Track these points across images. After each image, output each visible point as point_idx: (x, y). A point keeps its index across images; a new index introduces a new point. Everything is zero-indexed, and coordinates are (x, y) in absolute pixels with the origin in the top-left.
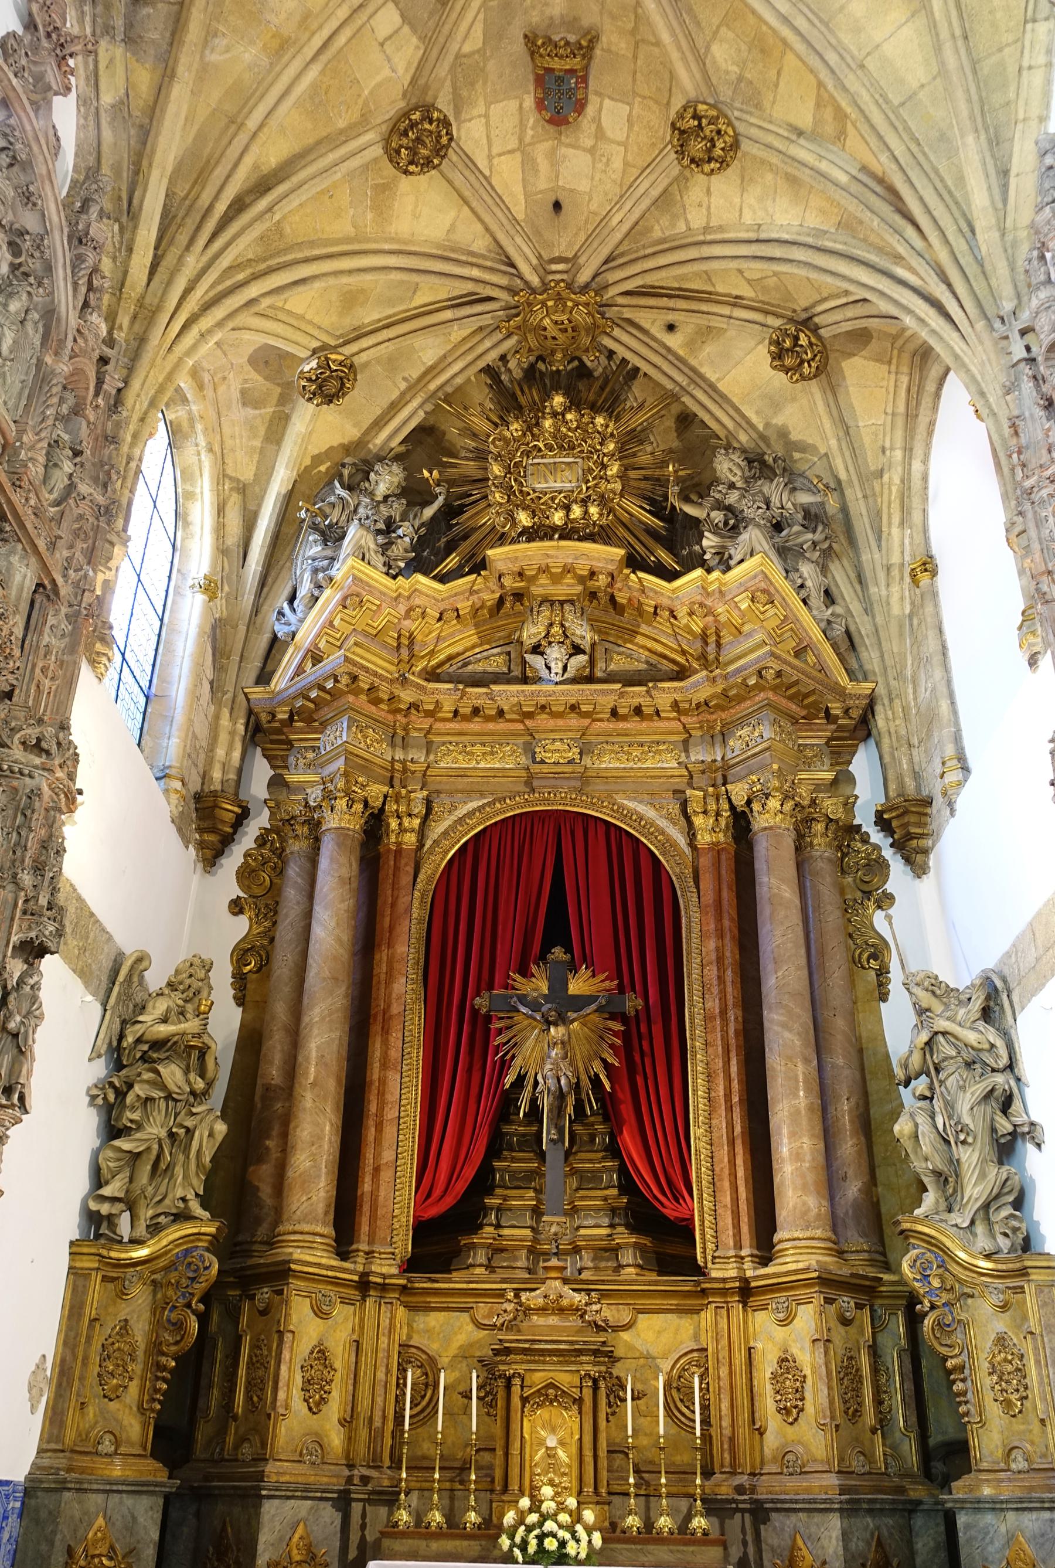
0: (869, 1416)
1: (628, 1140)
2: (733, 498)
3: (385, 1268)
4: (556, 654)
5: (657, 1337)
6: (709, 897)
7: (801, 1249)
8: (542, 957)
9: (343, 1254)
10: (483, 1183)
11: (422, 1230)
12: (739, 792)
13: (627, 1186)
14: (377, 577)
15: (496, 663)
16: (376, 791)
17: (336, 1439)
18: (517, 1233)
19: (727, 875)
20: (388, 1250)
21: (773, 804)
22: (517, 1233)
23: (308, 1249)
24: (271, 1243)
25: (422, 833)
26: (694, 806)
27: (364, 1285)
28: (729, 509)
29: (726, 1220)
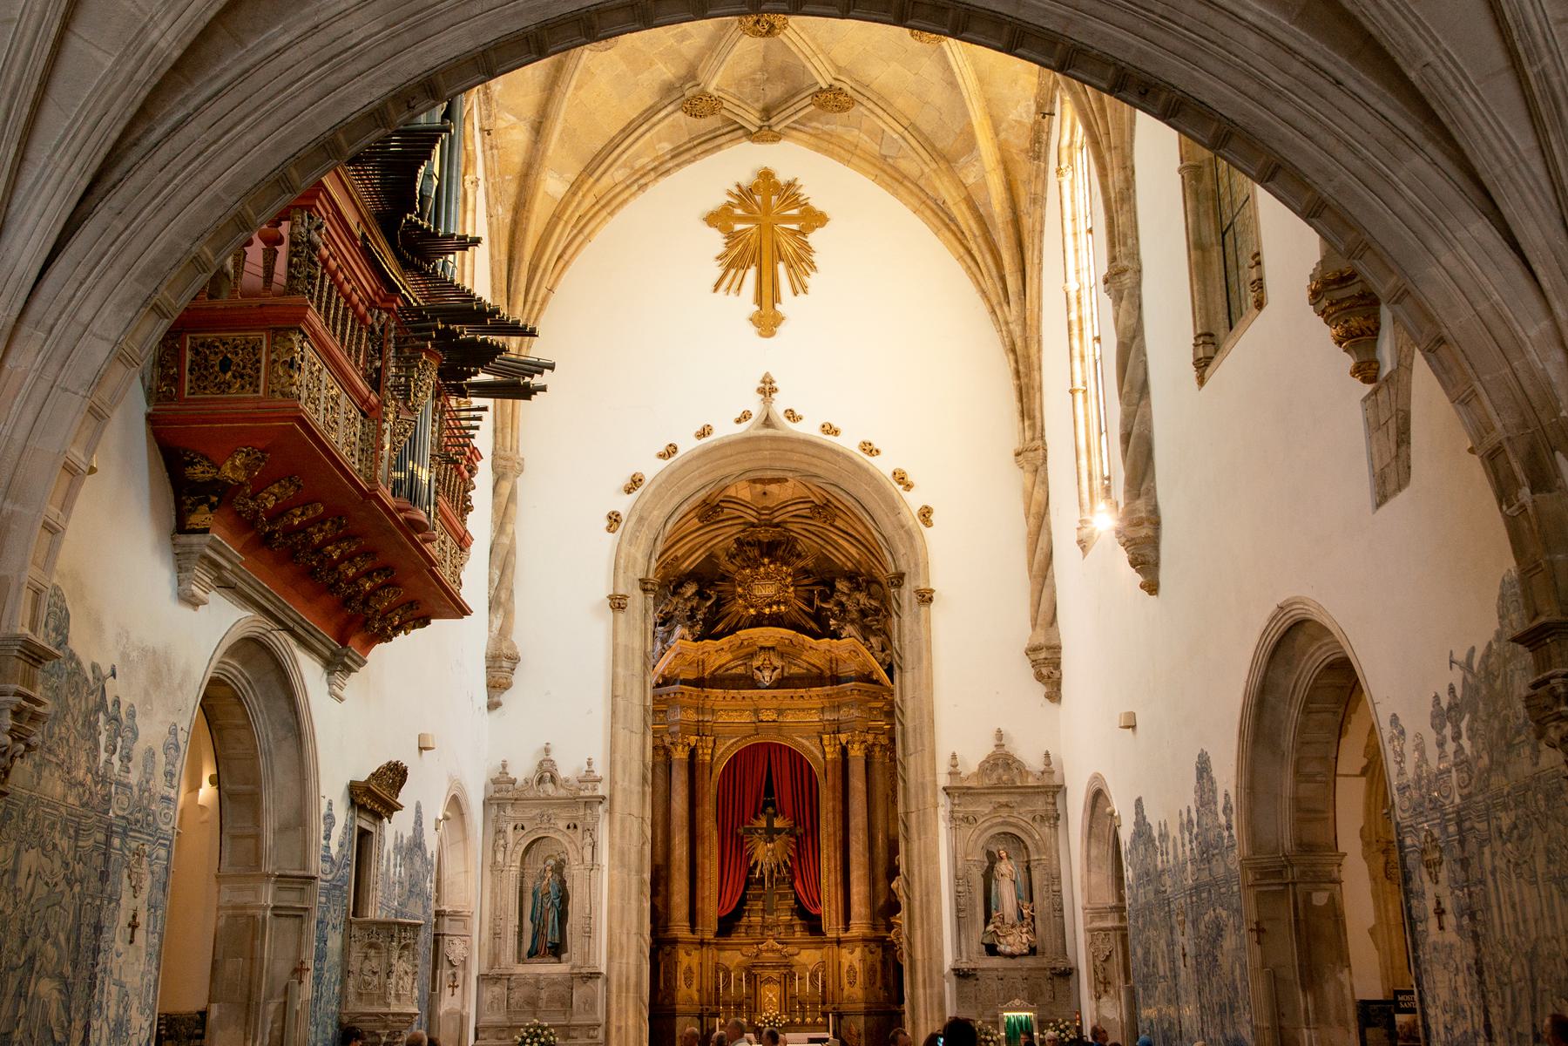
0: (878, 984)
1: (798, 884)
2: (844, 599)
3: (709, 936)
4: (767, 673)
5: (808, 957)
6: (830, 783)
7: (859, 927)
8: (763, 812)
9: (693, 931)
10: (743, 901)
11: (720, 920)
12: (843, 738)
13: (797, 901)
14: (690, 644)
15: (740, 670)
16: (693, 739)
17: (696, 996)
18: (756, 919)
19: (839, 773)
20: (709, 930)
21: (856, 746)
22: (756, 919)
23: (680, 928)
24: (666, 929)
25: (712, 755)
26: (826, 742)
27: (702, 943)
28: (840, 604)
29: (833, 915)
